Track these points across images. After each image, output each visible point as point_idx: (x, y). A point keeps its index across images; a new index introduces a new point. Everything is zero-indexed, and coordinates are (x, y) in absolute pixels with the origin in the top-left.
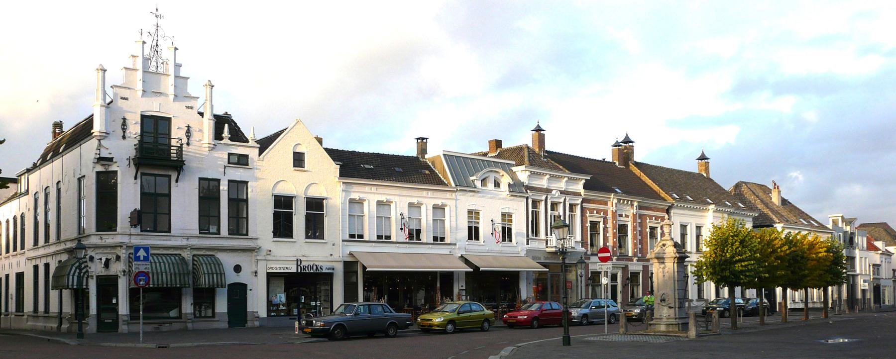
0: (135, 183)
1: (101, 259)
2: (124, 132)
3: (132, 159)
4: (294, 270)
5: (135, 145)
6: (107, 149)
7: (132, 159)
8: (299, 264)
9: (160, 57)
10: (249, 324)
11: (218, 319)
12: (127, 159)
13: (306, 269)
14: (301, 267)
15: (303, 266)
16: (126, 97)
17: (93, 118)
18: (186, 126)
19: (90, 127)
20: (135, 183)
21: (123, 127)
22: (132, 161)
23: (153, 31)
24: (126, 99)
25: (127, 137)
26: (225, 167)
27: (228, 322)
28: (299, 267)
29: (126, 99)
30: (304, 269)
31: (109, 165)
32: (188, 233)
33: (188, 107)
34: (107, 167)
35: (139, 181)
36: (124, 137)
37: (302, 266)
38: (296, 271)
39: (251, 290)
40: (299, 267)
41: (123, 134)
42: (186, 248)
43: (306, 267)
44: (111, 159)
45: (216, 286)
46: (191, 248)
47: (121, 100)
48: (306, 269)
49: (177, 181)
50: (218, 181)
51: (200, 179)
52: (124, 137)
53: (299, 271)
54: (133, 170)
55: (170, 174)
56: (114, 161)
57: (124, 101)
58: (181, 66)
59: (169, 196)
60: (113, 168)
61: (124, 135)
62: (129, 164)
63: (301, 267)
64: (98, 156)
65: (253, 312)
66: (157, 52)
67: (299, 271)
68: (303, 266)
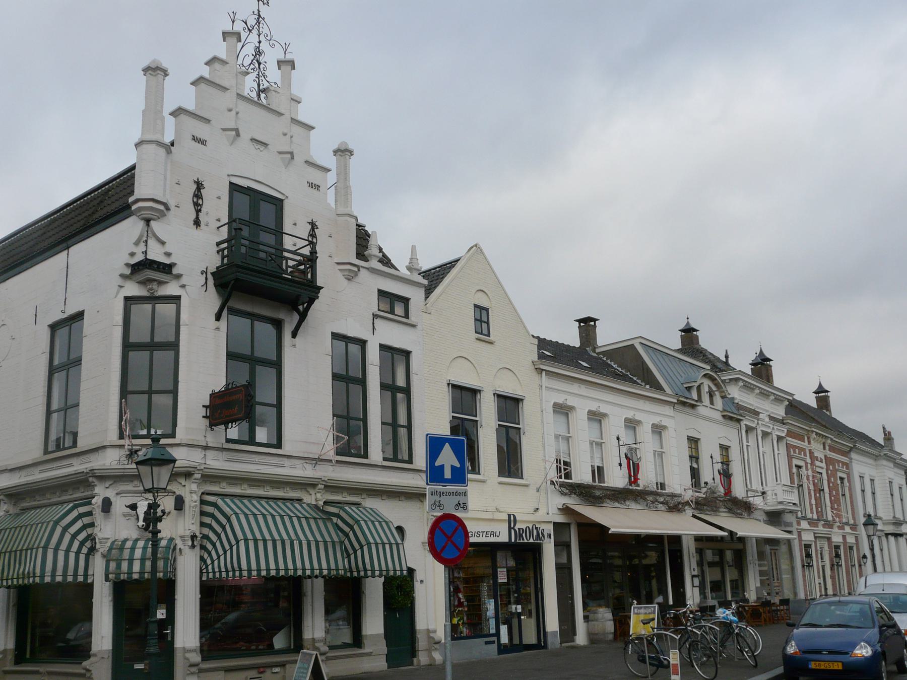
0: (218, 329)
1: (134, 507)
2: (198, 211)
3: (211, 273)
4: (504, 538)
5: (218, 244)
6: (163, 243)
7: (211, 273)
8: (512, 526)
9: (265, 76)
10: (423, 658)
11: (371, 651)
12: (202, 274)
13: (524, 535)
14: (515, 531)
15: (519, 529)
16: (203, 138)
17: (133, 176)
18: (309, 223)
19: (129, 184)
20: (218, 329)
21: (195, 200)
22: (210, 277)
23: (252, 21)
24: (203, 142)
25: (202, 224)
26: (375, 316)
27: (386, 655)
28: (513, 531)
29: (203, 142)
30: (521, 536)
31: (161, 283)
32: (314, 452)
33: (311, 185)
34: (154, 286)
35: (223, 324)
36: (197, 223)
37: (516, 528)
38: (507, 540)
39: (422, 581)
40: (513, 531)
41: (194, 216)
42: (314, 486)
43: (522, 529)
44: (167, 269)
45: (362, 574)
46: (325, 486)
47: (193, 141)
48: (524, 535)
49: (294, 335)
50: (363, 343)
51: (336, 336)
52: (197, 223)
53: (513, 540)
54: (213, 301)
55: (281, 316)
56: (175, 271)
57: (200, 145)
58: (299, 102)
59: (277, 365)
60: (171, 289)
61: (197, 217)
62: (206, 283)
63: (515, 531)
64: (139, 257)
65: (428, 631)
66: (259, 64)
67: (513, 540)
68: (519, 529)
